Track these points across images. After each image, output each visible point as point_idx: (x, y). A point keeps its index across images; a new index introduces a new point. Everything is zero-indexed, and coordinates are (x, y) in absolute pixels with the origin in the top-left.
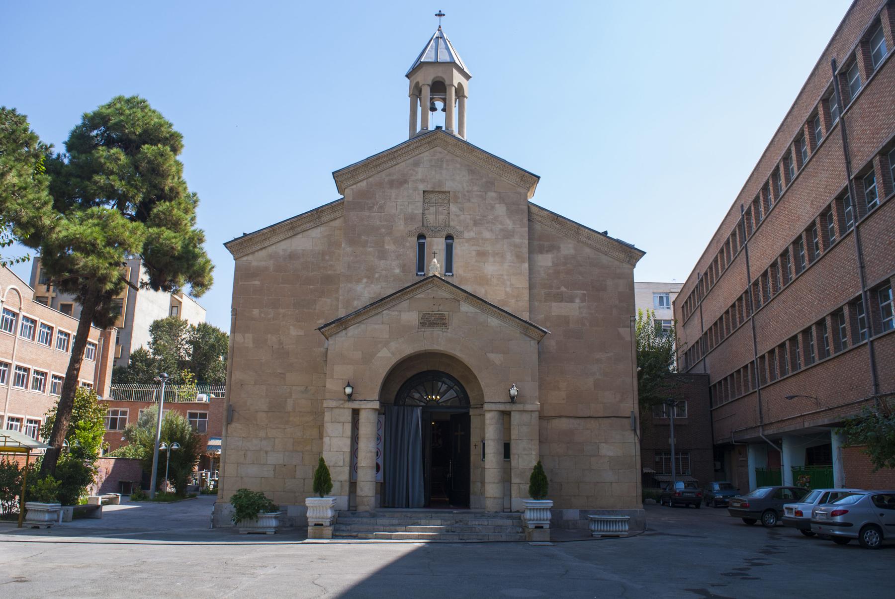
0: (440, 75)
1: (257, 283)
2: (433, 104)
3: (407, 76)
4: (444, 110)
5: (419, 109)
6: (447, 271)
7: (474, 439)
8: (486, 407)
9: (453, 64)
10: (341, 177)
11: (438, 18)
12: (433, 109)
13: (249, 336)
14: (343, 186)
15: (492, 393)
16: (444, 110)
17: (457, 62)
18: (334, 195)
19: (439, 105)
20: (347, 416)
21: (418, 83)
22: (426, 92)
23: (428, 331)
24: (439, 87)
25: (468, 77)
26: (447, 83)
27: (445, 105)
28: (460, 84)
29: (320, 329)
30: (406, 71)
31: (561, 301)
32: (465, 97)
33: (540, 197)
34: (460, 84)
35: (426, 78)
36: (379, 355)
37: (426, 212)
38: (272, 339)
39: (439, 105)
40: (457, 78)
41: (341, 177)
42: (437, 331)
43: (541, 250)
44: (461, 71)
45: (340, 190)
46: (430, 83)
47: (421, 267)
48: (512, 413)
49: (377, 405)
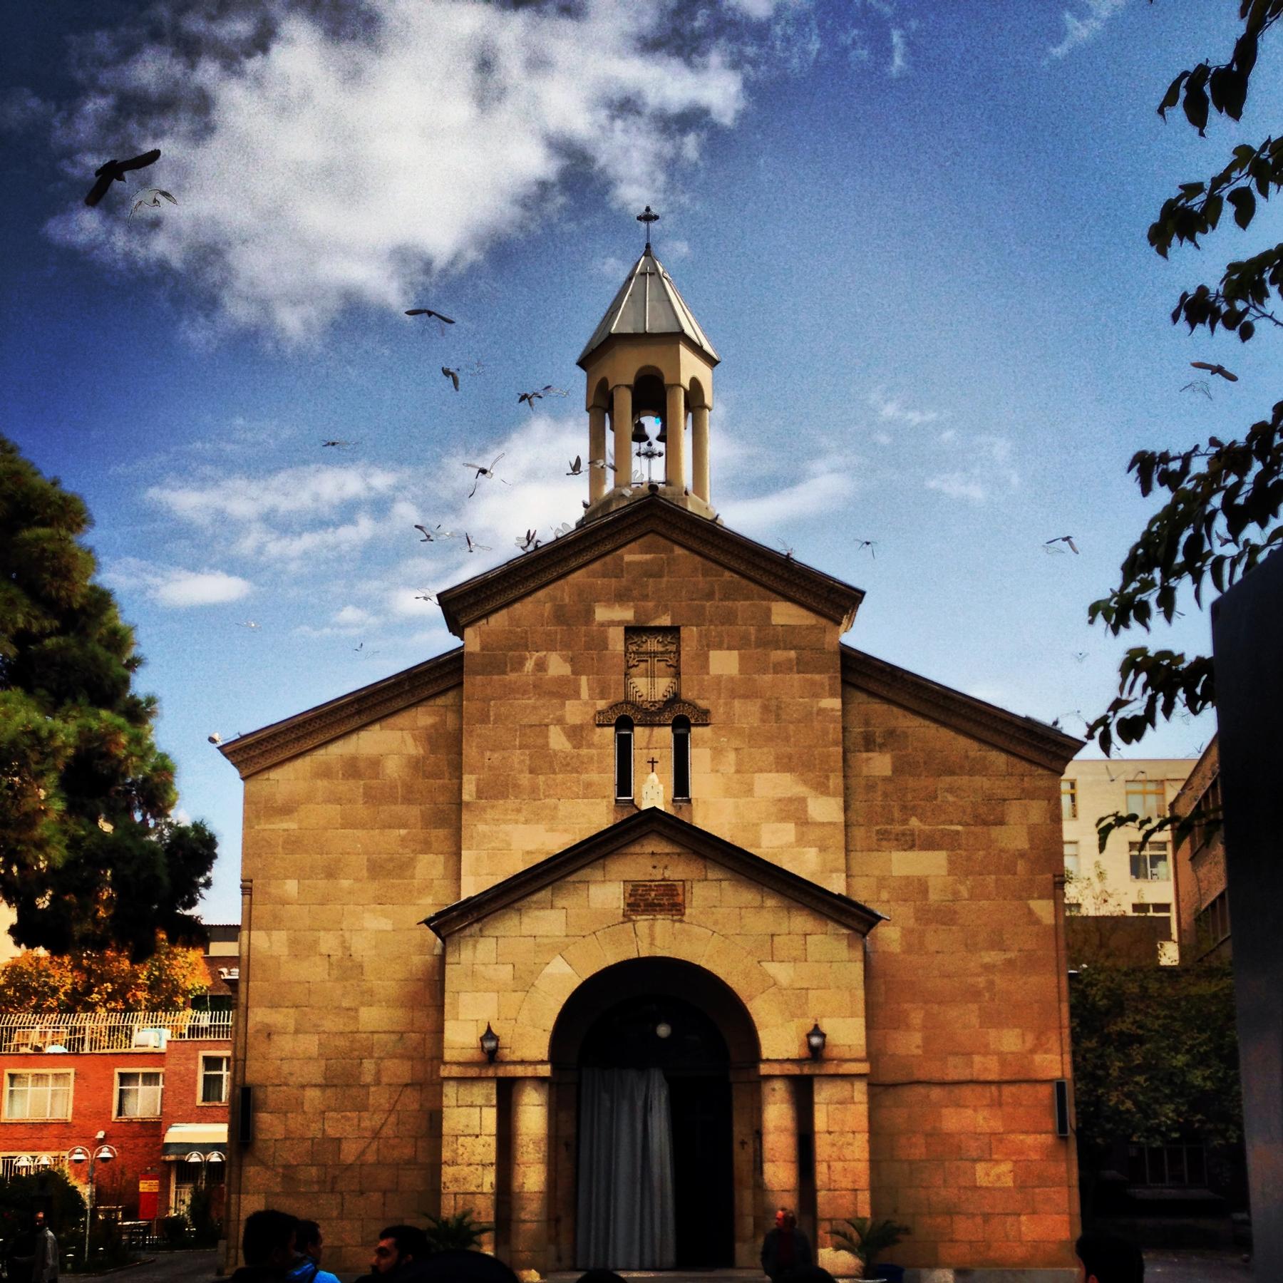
0: (651, 362)
1: (293, 826)
2: (640, 427)
3: (582, 363)
4: (661, 438)
5: (610, 437)
6: (676, 794)
7: (740, 1130)
8: (764, 1069)
9: (680, 336)
10: (460, 606)
11: (643, 225)
12: (640, 436)
13: (280, 937)
14: (463, 621)
15: (779, 1041)
16: (661, 438)
17: (688, 331)
18: (439, 641)
19: (652, 425)
20: (490, 1090)
21: (603, 383)
22: (624, 401)
23: (643, 922)
24: (652, 393)
25: (712, 362)
26: (667, 380)
27: (664, 428)
28: (695, 382)
29: (427, 922)
30: (577, 352)
31: (911, 847)
32: (704, 407)
33: (865, 634)
34: (695, 382)
35: (625, 369)
36: (548, 969)
37: (633, 671)
38: (328, 942)
39: (652, 425)
40: (690, 367)
41: (460, 606)
42: (663, 924)
43: (869, 743)
44: (697, 349)
45: (456, 627)
46: (630, 380)
47: (624, 785)
48: (816, 1080)
49: (545, 1070)
